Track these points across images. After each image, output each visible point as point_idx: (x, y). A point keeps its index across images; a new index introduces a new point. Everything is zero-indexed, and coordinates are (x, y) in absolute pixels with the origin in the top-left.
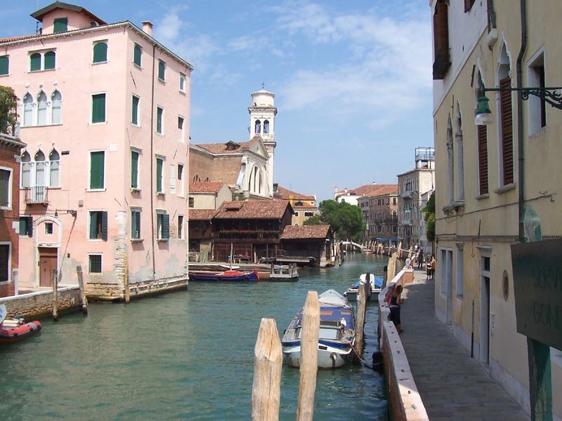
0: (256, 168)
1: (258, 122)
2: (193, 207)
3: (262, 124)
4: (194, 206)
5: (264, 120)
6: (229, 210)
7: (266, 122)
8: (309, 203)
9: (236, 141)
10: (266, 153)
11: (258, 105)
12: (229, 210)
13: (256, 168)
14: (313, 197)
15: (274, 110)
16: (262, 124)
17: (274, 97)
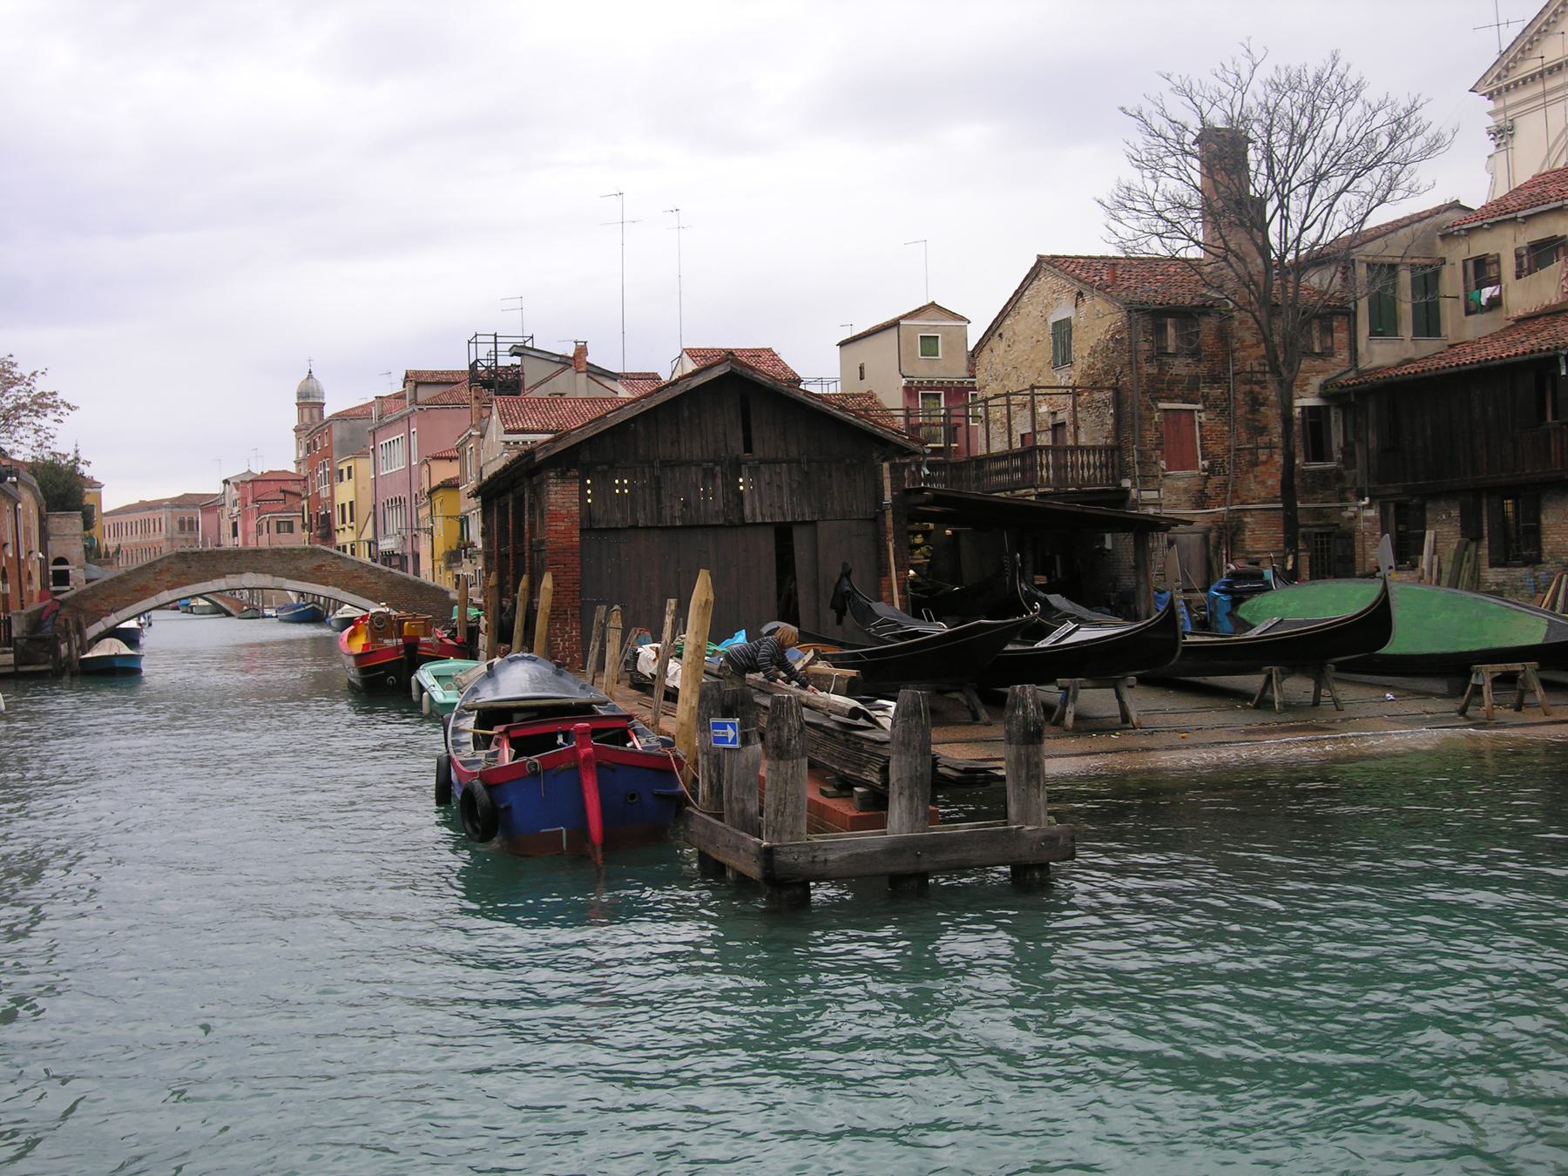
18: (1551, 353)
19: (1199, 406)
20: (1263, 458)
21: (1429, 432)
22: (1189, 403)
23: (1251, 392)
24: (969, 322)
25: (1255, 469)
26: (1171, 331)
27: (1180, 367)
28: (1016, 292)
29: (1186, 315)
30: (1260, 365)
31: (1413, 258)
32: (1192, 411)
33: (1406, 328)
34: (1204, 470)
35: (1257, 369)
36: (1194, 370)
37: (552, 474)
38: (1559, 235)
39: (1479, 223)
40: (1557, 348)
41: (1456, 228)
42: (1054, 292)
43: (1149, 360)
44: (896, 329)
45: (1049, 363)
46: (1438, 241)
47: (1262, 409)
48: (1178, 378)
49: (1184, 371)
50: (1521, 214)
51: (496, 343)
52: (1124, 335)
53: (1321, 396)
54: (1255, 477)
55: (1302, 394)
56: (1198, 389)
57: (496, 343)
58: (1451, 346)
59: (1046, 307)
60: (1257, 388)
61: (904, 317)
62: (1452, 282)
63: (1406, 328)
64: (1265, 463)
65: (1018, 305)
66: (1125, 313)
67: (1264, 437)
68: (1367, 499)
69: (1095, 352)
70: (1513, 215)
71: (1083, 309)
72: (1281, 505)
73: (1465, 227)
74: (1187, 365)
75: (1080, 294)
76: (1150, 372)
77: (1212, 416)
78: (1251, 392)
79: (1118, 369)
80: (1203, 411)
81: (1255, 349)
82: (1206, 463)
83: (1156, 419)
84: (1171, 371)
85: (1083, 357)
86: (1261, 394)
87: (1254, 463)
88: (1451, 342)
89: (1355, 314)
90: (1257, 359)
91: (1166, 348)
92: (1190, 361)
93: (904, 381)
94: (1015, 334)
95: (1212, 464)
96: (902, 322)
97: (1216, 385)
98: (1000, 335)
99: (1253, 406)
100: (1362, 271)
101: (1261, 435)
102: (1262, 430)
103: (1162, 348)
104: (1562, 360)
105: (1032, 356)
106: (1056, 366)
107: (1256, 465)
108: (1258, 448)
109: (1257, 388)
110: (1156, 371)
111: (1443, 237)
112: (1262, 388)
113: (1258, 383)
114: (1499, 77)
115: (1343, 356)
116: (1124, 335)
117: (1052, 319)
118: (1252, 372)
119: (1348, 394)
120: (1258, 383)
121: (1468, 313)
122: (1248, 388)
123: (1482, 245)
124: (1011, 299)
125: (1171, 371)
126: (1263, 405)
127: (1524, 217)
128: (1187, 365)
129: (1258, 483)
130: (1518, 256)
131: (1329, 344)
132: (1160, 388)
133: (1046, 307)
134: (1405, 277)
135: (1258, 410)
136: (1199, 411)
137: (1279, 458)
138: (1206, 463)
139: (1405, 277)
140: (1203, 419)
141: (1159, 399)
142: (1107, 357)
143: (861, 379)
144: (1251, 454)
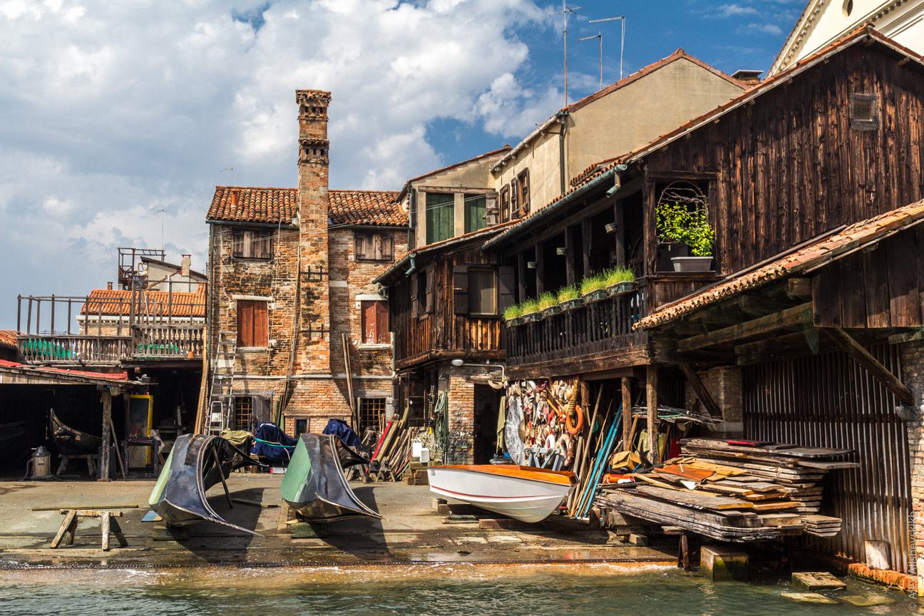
19: (270, 298)
22: (260, 295)
25: (308, 347)
26: (247, 241)
27: (255, 269)
29: (264, 229)
30: (317, 267)
31: (467, 189)
32: (265, 302)
34: (272, 347)
35: (313, 269)
36: (267, 271)
43: (228, 261)
46: (490, 176)
47: (316, 301)
48: (252, 276)
51: (133, 255)
54: (307, 353)
55: (361, 290)
56: (269, 285)
57: (133, 255)
60: (313, 285)
67: (317, 323)
72: (329, 376)
74: (261, 267)
76: (227, 271)
77: (282, 306)
78: (308, 288)
80: (273, 302)
81: (314, 255)
82: (273, 342)
83: (230, 307)
84: (246, 271)
86: (316, 289)
87: (308, 343)
89: (413, 231)
90: (314, 263)
91: (242, 253)
92: (264, 264)
95: (279, 342)
97: (286, 283)
99: (309, 298)
100: (422, 199)
101: (314, 321)
102: (318, 316)
103: (238, 253)
107: (308, 344)
108: (310, 331)
109: (313, 285)
110: (232, 270)
112: (318, 285)
118: (309, 273)
120: (317, 281)
122: (304, 285)
125: (246, 271)
126: (317, 298)
128: (261, 267)
129: (309, 358)
131: (388, 253)
132: (235, 284)
134: (459, 202)
135: (313, 302)
136: (269, 302)
137: (327, 339)
139: (459, 202)
141: (234, 292)
144: (304, 335)
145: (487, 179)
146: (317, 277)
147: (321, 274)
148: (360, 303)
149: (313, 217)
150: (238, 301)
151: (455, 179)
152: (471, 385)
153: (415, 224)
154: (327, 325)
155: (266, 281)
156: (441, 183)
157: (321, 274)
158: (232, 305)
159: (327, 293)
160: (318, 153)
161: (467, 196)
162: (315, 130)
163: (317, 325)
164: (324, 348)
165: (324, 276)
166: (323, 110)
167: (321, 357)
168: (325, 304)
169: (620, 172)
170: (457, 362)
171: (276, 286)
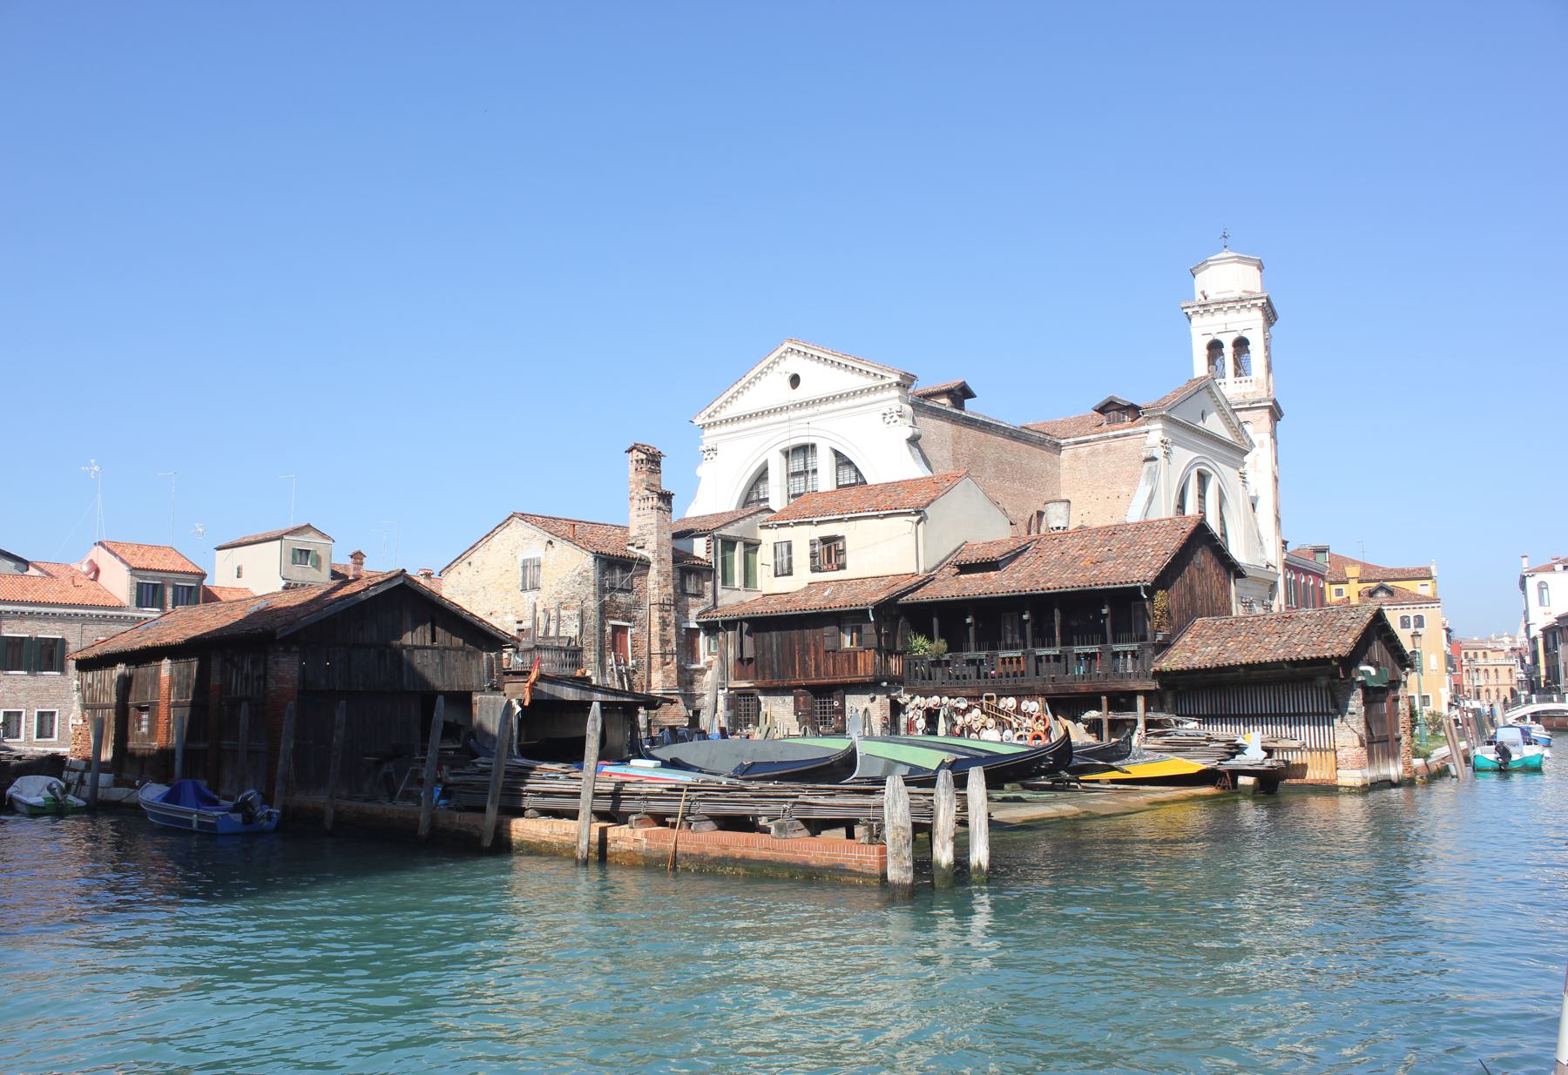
0: (1203, 478)
1: (1215, 347)
2: (842, 567)
3: (1228, 351)
4: (850, 559)
5: (1234, 336)
6: (965, 568)
7: (1241, 344)
8: (1415, 587)
9: (1126, 397)
10: (1238, 429)
11: (1212, 297)
12: (965, 568)
13: (1203, 478)
14: (1428, 570)
15: (1260, 303)
16: (1228, 351)
17: (1261, 268)
18: (863, 608)
20: (668, 660)
21: (775, 648)
23: (663, 617)
24: (334, 542)
28: (488, 535)
32: (626, 627)
33: (738, 581)
35: (666, 602)
37: (281, 649)
38: (840, 535)
39: (787, 522)
40: (867, 604)
41: (771, 523)
42: (524, 539)
44: (279, 541)
45: (517, 587)
49: (623, 601)
50: (815, 520)
52: (590, 574)
53: (697, 623)
54: (664, 672)
58: (764, 595)
59: (516, 548)
60: (666, 614)
61: (287, 534)
62: (765, 556)
63: (738, 581)
64: (668, 664)
65: (488, 544)
66: (592, 559)
68: (726, 690)
69: (563, 583)
70: (810, 520)
71: (552, 552)
72: (678, 692)
73: (777, 522)
75: (550, 542)
78: (663, 617)
79: (583, 597)
82: (634, 662)
85: (551, 586)
88: (764, 593)
93: (283, 583)
94: (483, 563)
96: (285, 537)
98: (470, 563)
100: (719, 545)
101: (667, 645)
104: (870, 612)
105: (500, 581)
106: (524, 590)
111: (760, 527)
113: (666, 611)
114: (709, 416)
115: (709, 596)
116: (590, 574)
117: (520, 559)
119: (718, 622)
121: (776, 575)
123: (784, 534)
124: (483, 539)
126: (668, 626)
127: (817, 522)
130: (813, 544)
133: (516, 548)
134: (739, 548)
137: (675, 660)
138: (634, 662)
139: (739, 548)
140: (633, 632)
142: (574, 587)
143: (238, 577)
144: (662, 657)
145: (756, 531)
146: (668, 608)
147: (670, 605)
148: (684, 630)
149: (664, 556)
150: (613, 626)
151: (738, 530)
152: (888, 700)
153: (716, 565)
154: (675, 649)
155: (630, 607)
156: (729, 532)
157: (670, 605)
158: (609, 629)
159: (673, 621)
160: (666, 501)
161: (747, 545)
162: (653, 479)
163: (668, 648)
164: (672, 668)
165: (672, 607)
166: (658, 464)
167: (672, 675)
168: (674, 631)
169: (1145, 587)
170: (885, 684)
171: (635, 614)
